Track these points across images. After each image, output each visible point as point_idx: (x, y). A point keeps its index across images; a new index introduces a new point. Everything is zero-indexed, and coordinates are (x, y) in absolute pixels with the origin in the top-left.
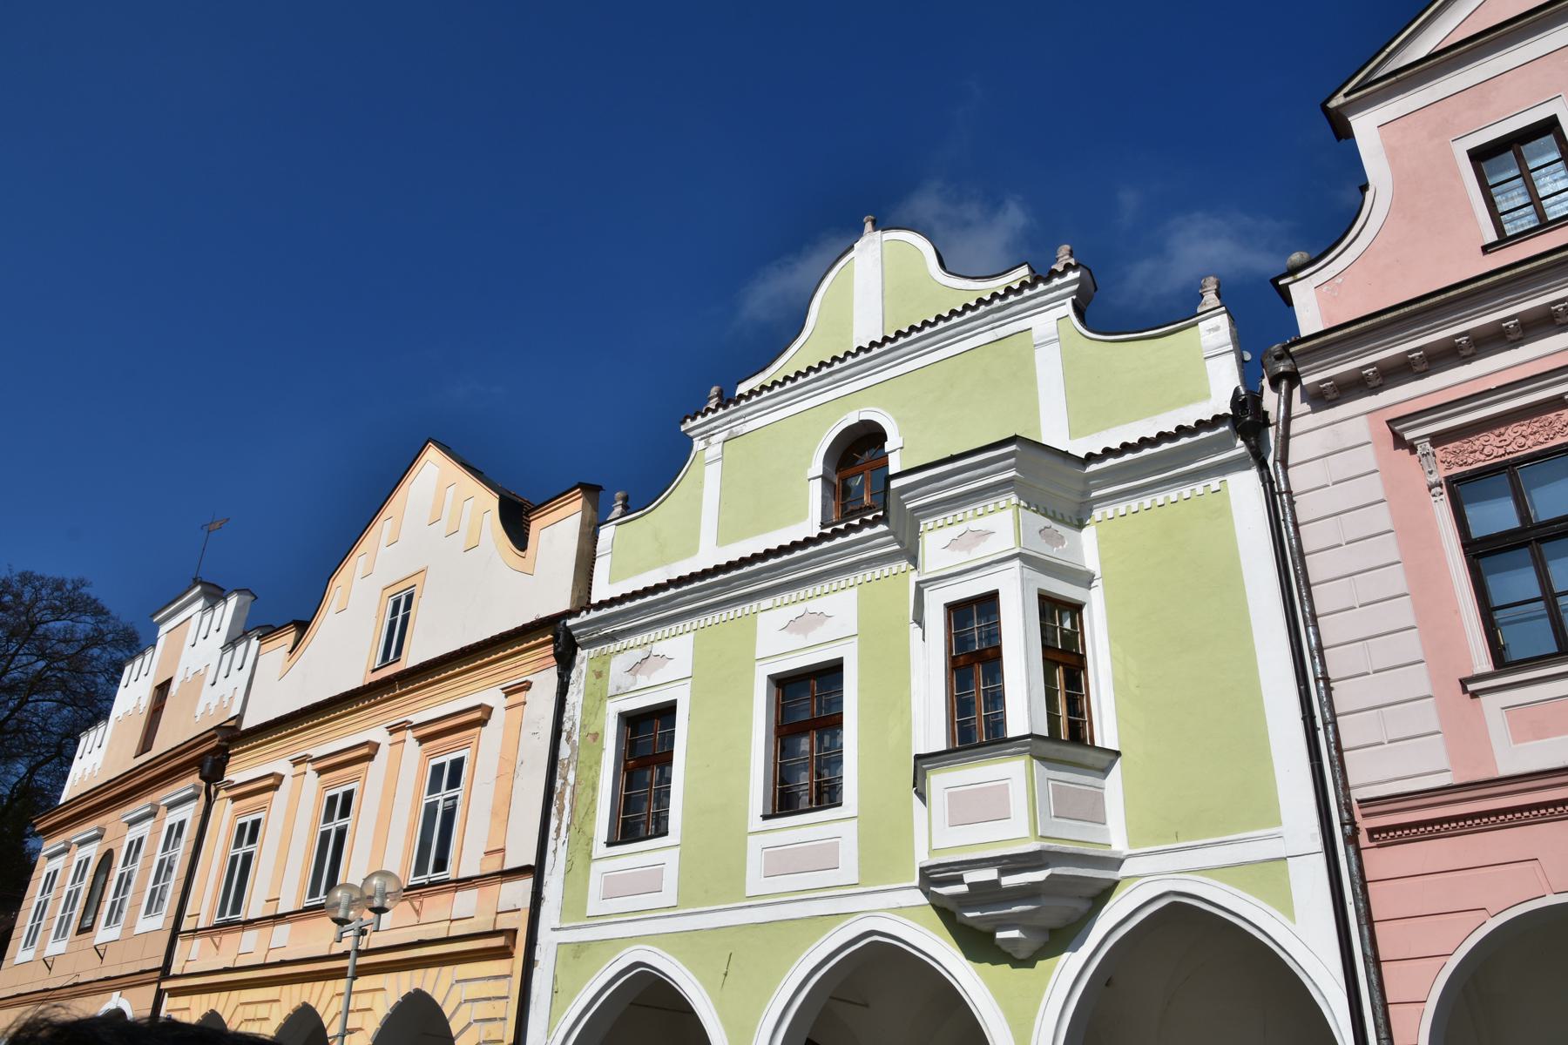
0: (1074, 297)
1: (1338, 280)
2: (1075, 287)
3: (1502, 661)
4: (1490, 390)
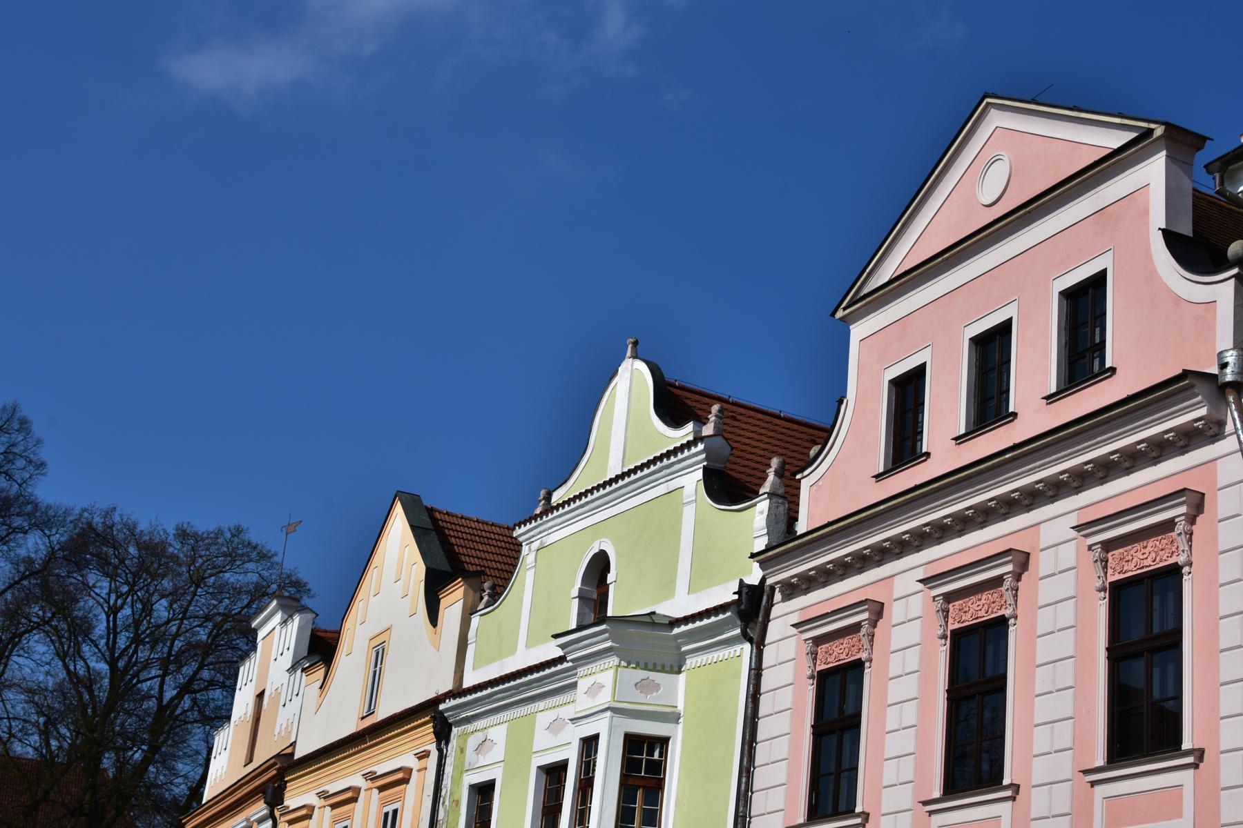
0: (705, 463)
1: (820, 483)
2: (703, 456)
4: (828, 613)
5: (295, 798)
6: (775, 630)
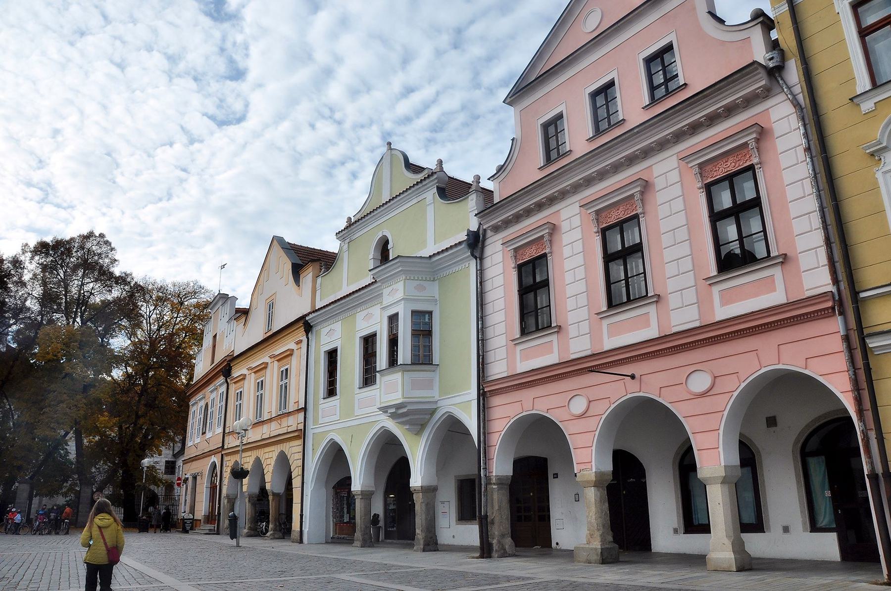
1: (505, 179)
2: (436, 181)
3: (611, 305)
5: (236, 373)
6: (488, 251)
